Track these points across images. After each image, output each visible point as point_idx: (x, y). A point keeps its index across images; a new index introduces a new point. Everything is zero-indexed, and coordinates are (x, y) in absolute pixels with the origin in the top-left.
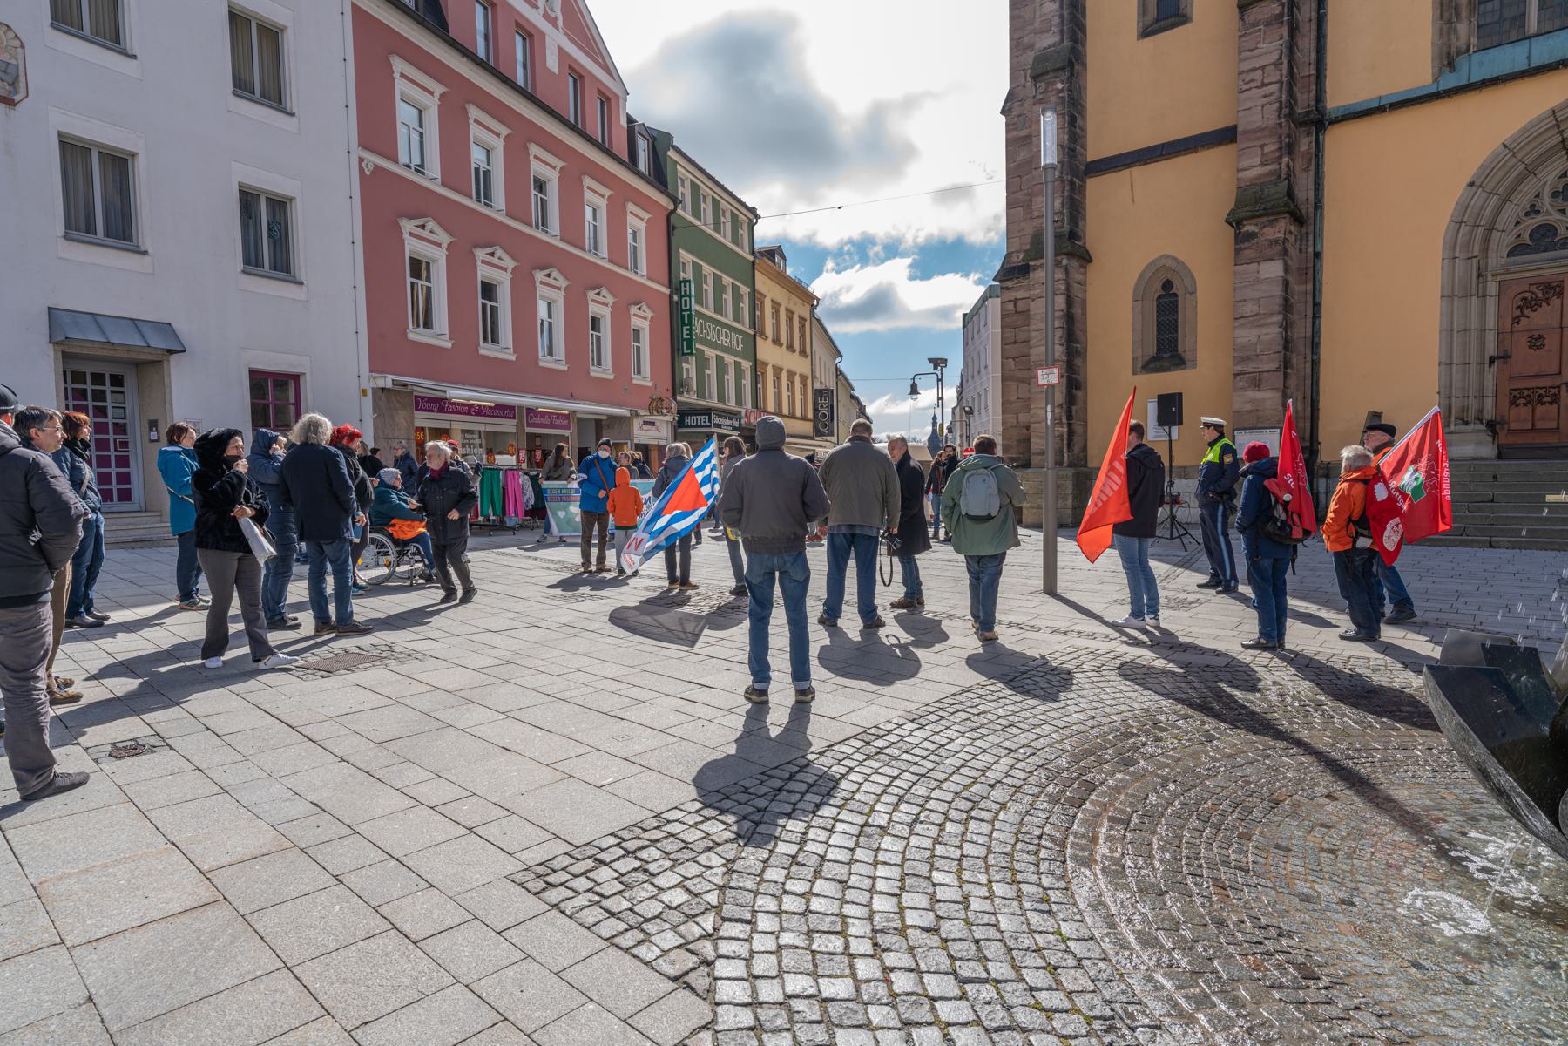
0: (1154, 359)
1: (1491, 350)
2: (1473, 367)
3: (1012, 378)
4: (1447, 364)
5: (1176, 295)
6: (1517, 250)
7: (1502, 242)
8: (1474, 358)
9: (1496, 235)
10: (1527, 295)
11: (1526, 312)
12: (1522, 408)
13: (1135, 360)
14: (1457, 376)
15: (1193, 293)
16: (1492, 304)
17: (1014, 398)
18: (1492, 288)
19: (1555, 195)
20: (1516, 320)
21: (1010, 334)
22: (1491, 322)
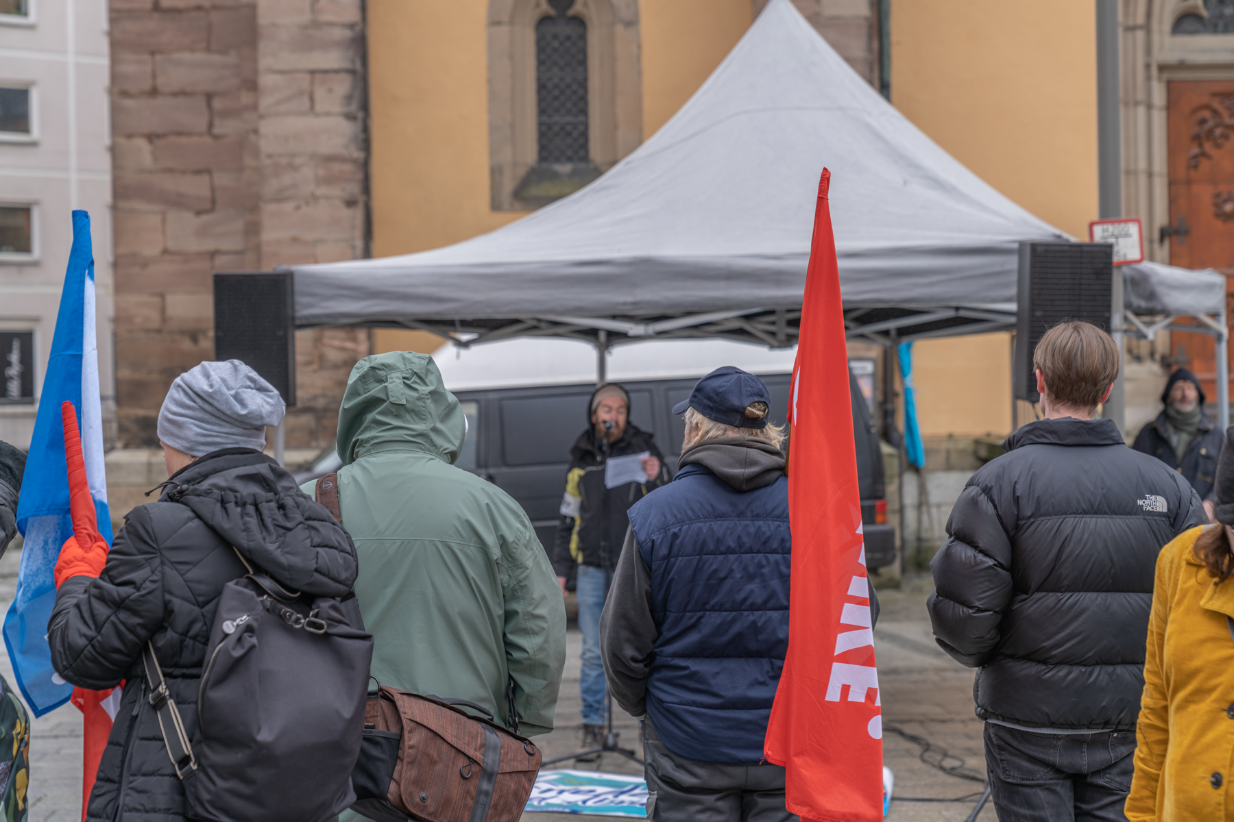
0: (535, 176)
1: (1161, 218)
3: (145, 193)
5: (580, 21)
10: (1206, 114)
11: (1208, 147)
13: (496, 172)
15: (632, 23)
17: (150, 250)
18: (1159, 96)
20: (1194, 164)
21: (135, 67)
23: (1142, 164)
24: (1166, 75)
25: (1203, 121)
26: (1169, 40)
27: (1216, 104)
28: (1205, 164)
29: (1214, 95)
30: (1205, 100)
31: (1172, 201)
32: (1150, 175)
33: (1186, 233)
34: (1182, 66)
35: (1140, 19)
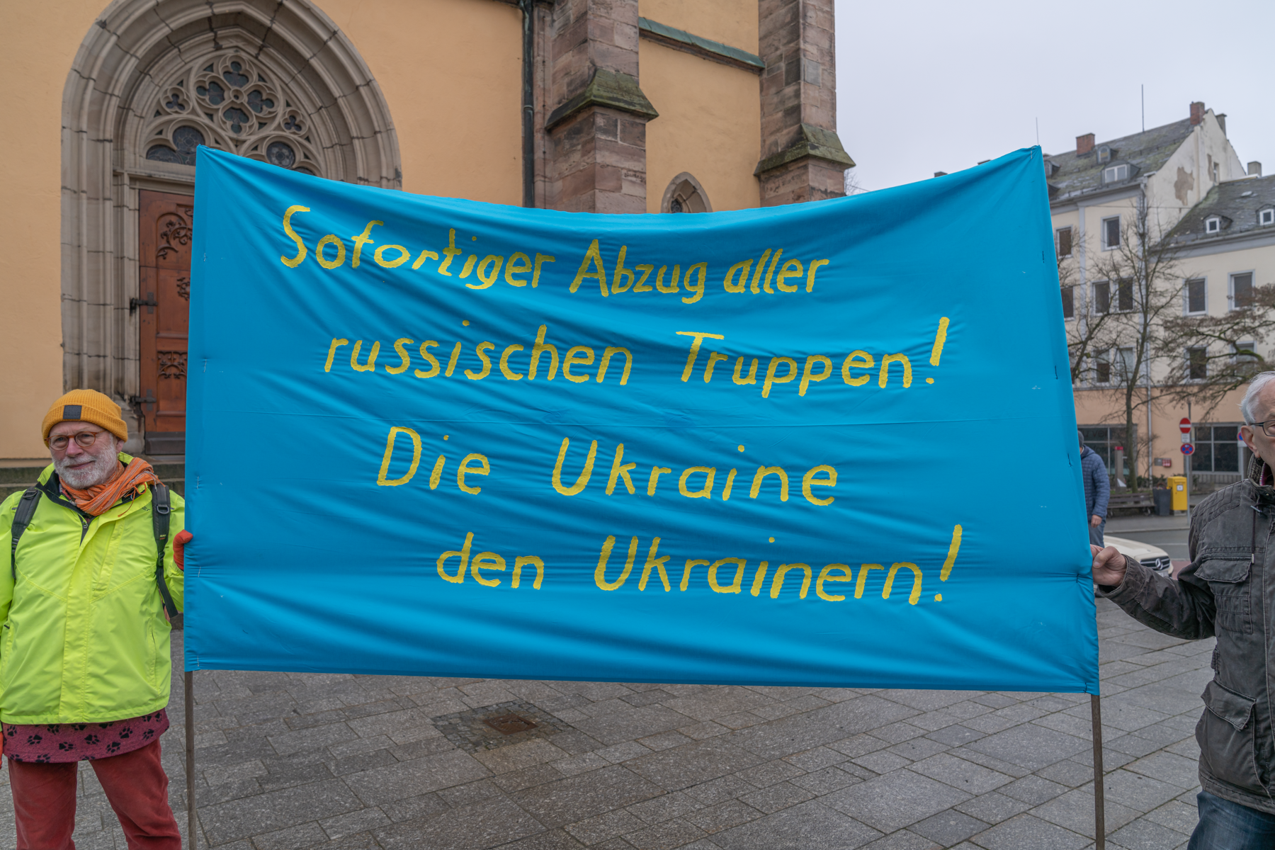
1: (132, 290)
2: (110, 312)
4: (74, 300)
6: (157, 149)
7: (140, 132)
8: (110, 299)
9: (132, 120)
10: (174, 219)
11: (174, 243)
12: (174, 382)
14: (87, 323)
16: (131, 221)
18: (131, 198)
19: (201, 89)
20: (162, 253)
22: (131, 248)
23: (110, 246)
24: (138, 186)
25: (171, 224)
26: (143, 161)
27: (181, 212)
28: (171, 254)
29: (179, 205)
30: (173, 208)
31: (142, 280)
32: (120, 258)
33: (155, 305)
34: (149, 179)
35: (109, 134)
